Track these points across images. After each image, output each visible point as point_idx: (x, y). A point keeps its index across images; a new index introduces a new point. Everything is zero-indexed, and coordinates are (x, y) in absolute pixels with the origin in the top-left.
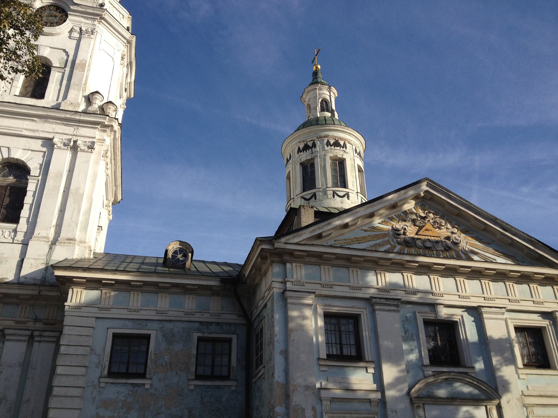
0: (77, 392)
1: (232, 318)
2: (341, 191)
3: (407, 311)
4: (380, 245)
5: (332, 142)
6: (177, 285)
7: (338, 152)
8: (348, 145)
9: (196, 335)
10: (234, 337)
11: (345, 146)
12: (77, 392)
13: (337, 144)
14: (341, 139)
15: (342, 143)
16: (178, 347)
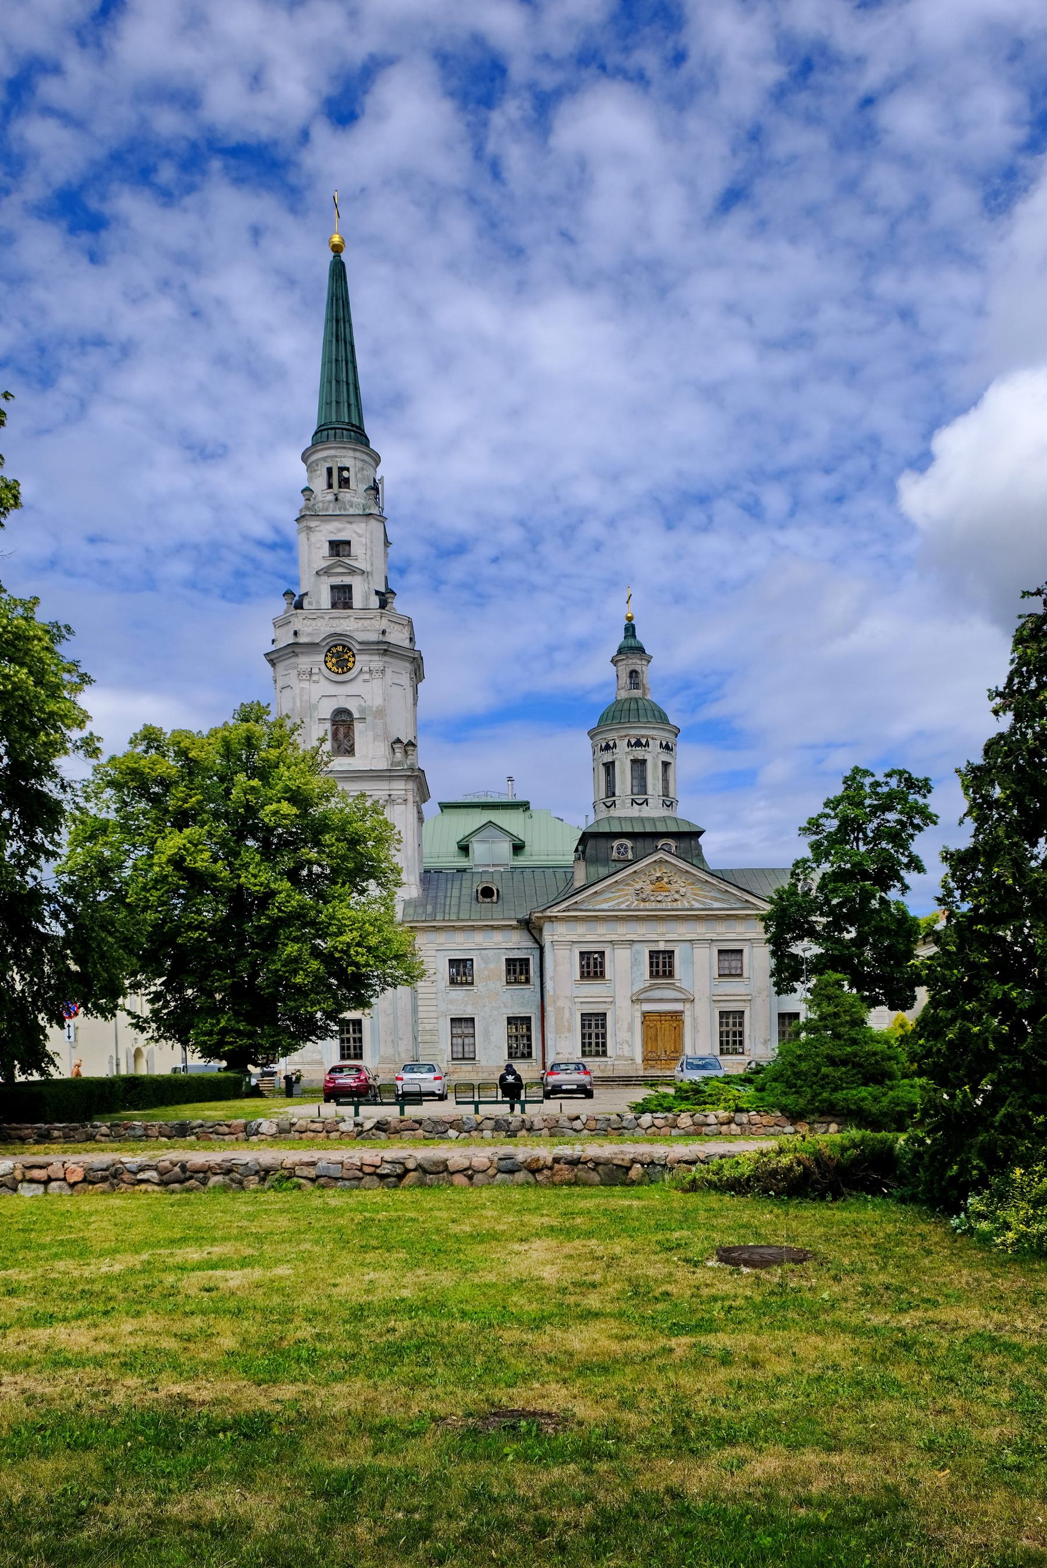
0: (433, 996)
1: (530, 944)
2: (640, 798)
3: (637, 946)
4: (623, 903)
5: (633, 741)
6: (487, 926)
7: (639, 753)
8: (651, 742)
9: (504, 958)
10: (531, 958)
11: (647, 744)
12: (433, 996)
13: (638, 744)
14: (643, 736)
15: (644, 741)
16: (492, 966)
